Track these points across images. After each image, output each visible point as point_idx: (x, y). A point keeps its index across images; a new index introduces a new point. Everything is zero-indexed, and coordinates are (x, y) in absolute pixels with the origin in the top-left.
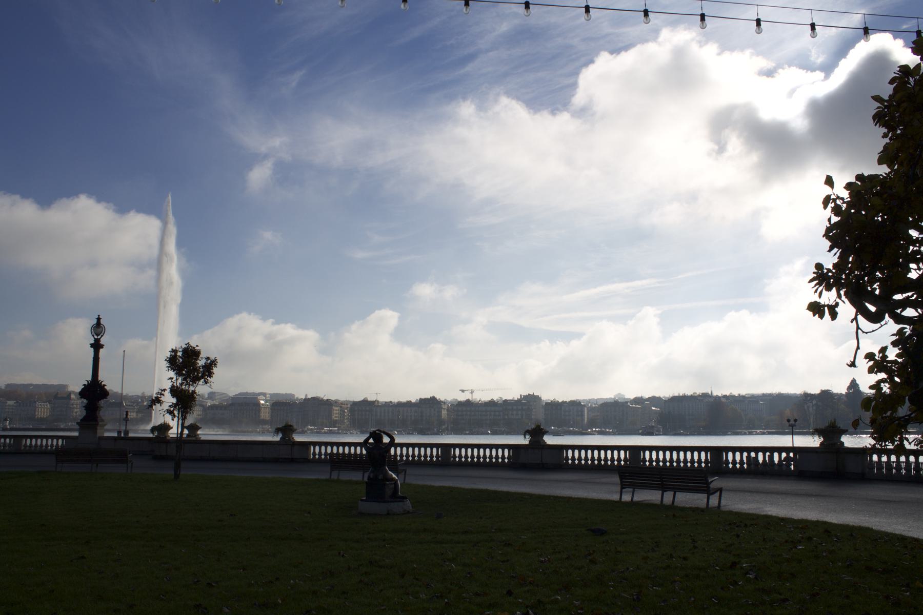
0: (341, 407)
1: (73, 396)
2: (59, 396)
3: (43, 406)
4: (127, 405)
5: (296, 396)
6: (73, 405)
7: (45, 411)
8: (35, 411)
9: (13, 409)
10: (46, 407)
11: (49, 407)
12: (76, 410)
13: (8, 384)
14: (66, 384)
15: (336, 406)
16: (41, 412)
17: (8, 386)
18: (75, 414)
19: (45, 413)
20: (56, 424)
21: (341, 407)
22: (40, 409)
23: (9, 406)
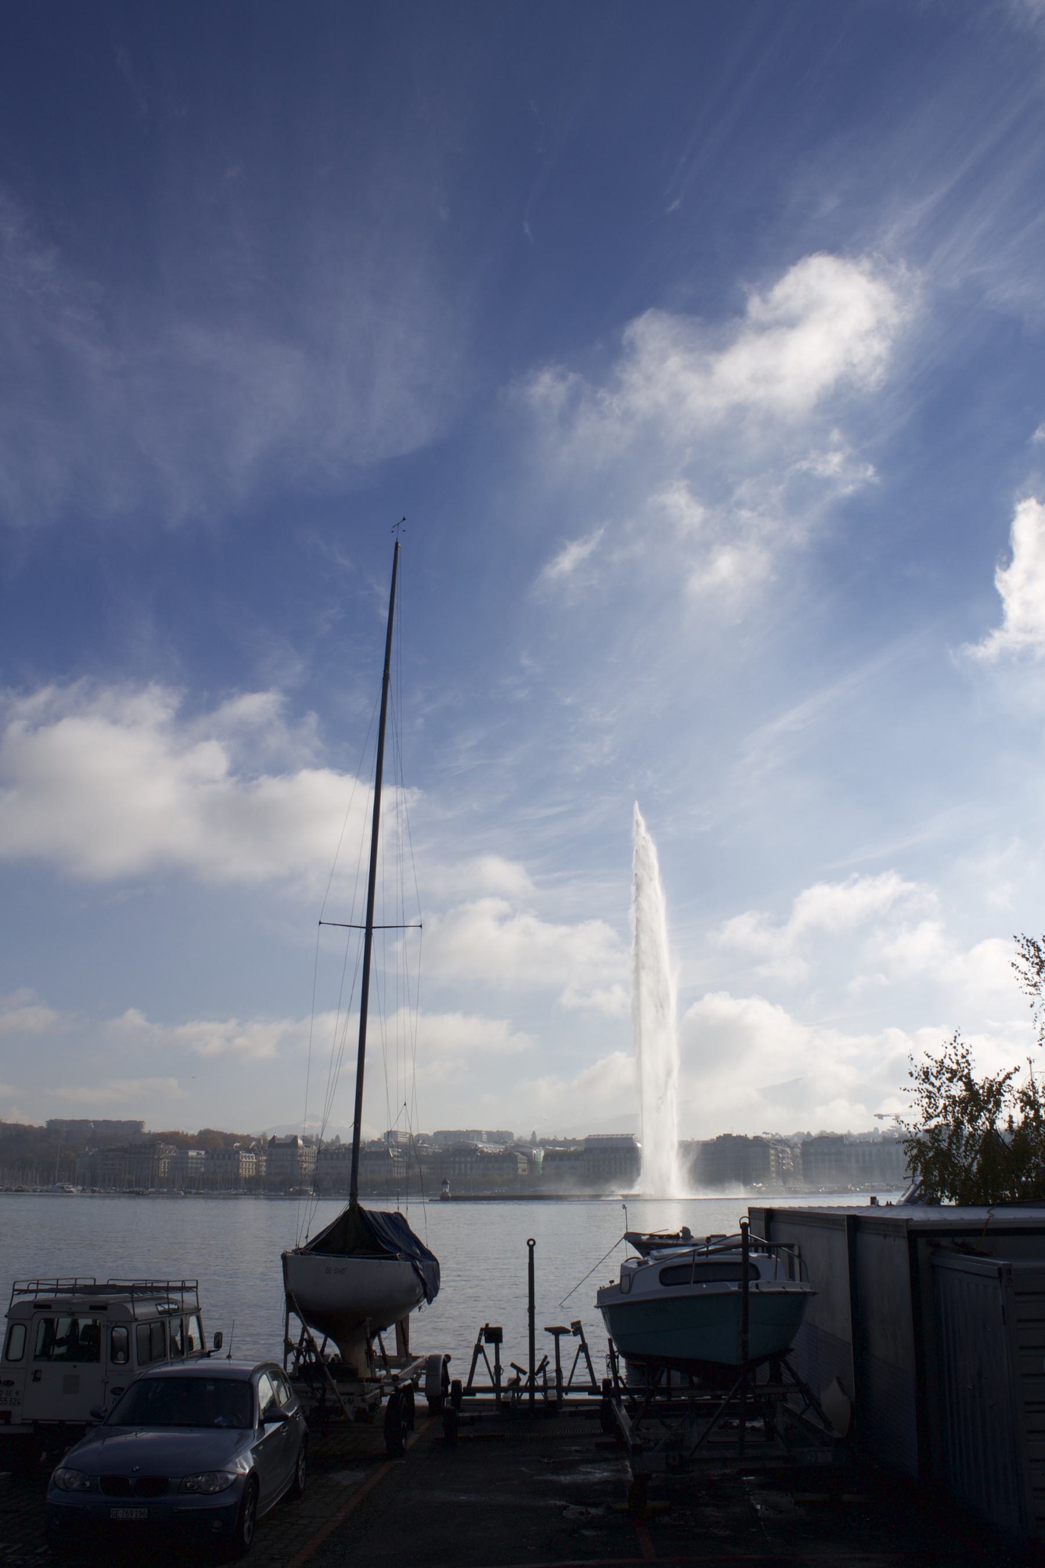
0: (776, 1149)
1: (300, 1142)
2: (277, 1142)
3: (248, 1160)
4: (394, 1156)
5: (515, 1138)
6: (301, 1156)
7: (251, 1167)
8: (238, 1167)
9: (197, 1163)
10: (251, 1160)
11: (255, 1160)
12: (305, 1165)
13: (51, 1121)
14: (142, 1120)
15: (772, 1148)
16: (246, 1169)
17: (50, 1123)
18: (303, 1171)
19: (251, 1170)
20: (297, 1188)
21: (776, 1149)
22: (244, 1163)
23: (192, 1158)
